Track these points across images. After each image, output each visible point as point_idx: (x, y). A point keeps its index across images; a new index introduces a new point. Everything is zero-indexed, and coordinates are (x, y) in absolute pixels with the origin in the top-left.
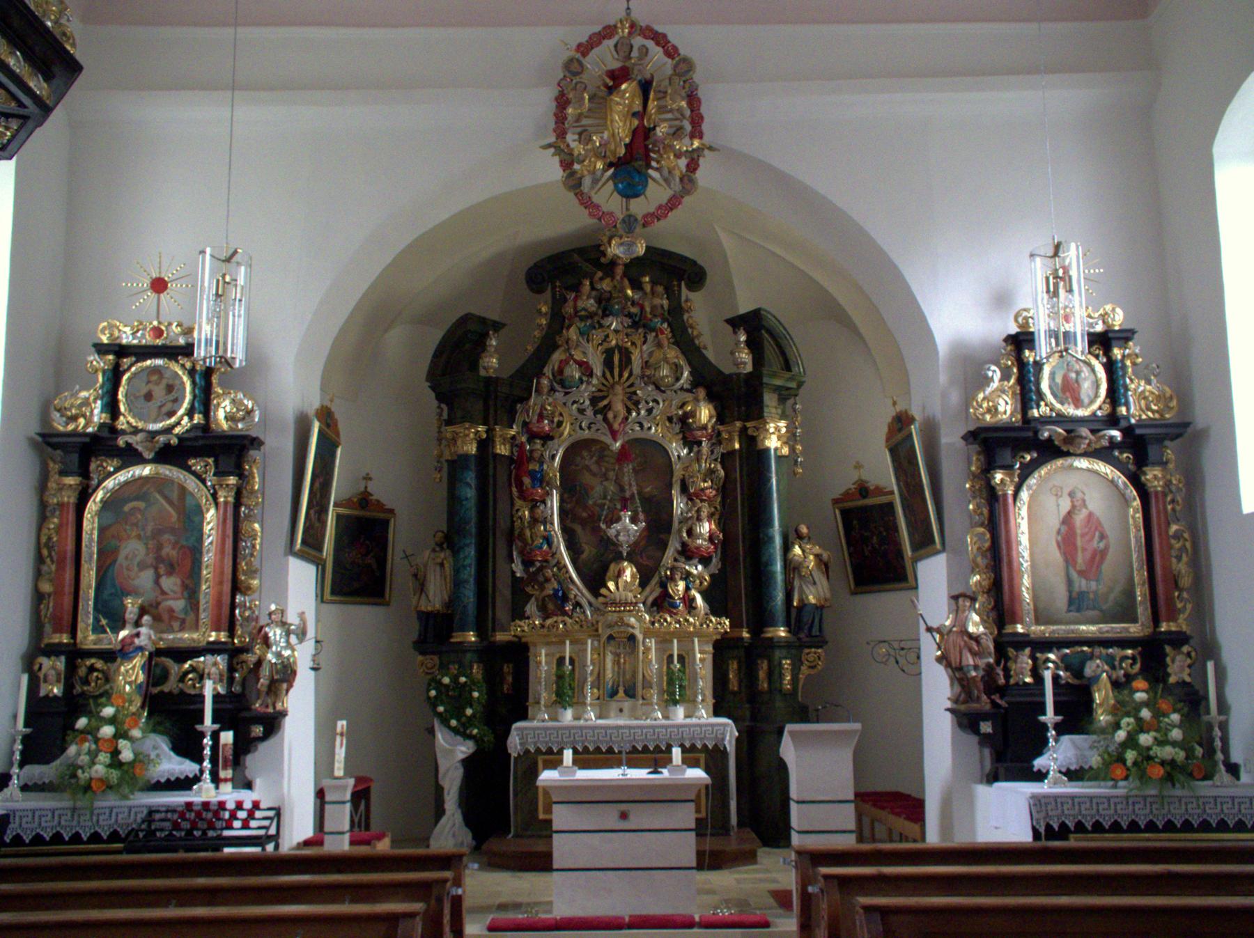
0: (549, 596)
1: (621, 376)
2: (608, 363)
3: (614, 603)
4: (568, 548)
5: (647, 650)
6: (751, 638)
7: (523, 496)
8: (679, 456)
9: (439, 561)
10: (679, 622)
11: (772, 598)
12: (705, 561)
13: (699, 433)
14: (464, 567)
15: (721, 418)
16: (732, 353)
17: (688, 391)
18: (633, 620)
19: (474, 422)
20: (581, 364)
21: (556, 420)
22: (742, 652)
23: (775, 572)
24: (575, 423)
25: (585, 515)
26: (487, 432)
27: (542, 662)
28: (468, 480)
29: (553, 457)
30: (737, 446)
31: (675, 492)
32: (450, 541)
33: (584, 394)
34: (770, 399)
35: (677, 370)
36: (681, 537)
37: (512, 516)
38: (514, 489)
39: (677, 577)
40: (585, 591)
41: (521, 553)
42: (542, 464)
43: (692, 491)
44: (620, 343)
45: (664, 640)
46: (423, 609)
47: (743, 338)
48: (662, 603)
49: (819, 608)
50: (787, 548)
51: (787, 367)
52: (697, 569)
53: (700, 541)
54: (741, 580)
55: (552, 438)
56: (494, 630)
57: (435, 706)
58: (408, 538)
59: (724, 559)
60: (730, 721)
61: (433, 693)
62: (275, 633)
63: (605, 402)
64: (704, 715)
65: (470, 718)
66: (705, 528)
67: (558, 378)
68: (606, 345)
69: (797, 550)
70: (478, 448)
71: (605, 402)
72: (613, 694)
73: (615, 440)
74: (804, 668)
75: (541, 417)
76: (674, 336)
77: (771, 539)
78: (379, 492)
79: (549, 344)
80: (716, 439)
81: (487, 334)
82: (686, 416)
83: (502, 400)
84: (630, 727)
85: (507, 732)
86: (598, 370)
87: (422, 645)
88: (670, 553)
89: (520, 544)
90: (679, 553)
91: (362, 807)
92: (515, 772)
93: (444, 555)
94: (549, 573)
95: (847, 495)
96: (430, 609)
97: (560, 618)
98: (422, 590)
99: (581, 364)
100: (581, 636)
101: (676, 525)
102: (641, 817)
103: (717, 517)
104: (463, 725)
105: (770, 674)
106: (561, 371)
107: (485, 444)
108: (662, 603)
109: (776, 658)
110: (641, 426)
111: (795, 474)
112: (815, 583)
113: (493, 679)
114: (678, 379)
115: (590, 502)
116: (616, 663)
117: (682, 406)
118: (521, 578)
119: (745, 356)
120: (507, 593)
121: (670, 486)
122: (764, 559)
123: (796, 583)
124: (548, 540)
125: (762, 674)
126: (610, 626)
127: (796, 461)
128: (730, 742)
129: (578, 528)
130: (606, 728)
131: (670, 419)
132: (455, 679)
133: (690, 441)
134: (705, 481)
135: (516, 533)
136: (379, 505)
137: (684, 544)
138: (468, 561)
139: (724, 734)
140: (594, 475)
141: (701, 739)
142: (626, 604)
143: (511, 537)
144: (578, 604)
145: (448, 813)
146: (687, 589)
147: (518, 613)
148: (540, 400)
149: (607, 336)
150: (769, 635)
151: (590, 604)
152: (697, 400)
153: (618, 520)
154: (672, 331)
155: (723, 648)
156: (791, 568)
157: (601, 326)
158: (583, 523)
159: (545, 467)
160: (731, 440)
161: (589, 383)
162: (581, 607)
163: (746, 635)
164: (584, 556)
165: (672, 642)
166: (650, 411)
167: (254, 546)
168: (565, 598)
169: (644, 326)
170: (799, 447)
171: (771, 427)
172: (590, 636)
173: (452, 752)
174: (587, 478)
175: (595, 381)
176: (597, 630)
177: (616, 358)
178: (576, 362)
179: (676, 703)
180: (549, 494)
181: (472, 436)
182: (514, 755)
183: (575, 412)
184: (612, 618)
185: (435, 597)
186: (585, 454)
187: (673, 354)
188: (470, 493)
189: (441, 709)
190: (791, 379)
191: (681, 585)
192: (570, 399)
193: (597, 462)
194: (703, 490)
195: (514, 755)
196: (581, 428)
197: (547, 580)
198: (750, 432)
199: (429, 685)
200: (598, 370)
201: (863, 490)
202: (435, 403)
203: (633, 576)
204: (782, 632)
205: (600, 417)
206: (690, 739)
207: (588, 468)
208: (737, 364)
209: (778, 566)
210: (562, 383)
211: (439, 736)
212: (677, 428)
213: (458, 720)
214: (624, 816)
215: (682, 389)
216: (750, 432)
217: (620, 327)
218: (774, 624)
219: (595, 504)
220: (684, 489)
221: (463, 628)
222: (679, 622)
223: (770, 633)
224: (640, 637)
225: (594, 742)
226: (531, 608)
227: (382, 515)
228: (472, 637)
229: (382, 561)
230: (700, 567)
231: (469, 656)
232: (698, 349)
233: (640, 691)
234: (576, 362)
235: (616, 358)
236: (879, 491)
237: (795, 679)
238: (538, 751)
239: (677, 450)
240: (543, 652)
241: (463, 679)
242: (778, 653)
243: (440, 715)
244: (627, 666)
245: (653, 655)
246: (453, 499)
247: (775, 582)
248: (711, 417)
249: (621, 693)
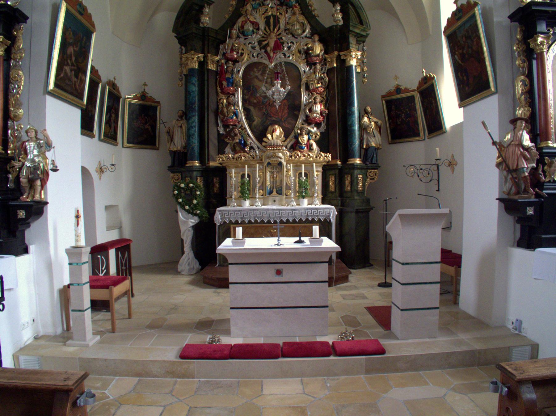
0: (237, 143)
1: (274, 30)
2: (267, 23)
3: (271, 146)
4: (247, 119)
5: (288, 170)
6: (342, 164)
7: (223, 92)
8: (304, 71)
9: (180, 125)
10: (304, 156)
11: (352, 143)
12: (318, 125)
13: (315, 59)
14: (192, 127)
15: (326, 52)
16: (333, 15)
17: (308, 38)
18: (281, 155)
19: (197, 51)
20: (253, 23)
21: (240, 52)
22: (337, 171)
23: (354, 131)
24: (251, 54)
25: (255, 101)
26: (204, 57)
27: (233, 176)
28: (194, 82)
29: (239, 71)
30: (335, 65)
31: (303, 89)
32: (185, 115)
33: (255, 38)
34: (352, 40)
35: (303, 25)
36: (305, 113)
37: (217, 102)
38: (219, 89)
39: (304, 133)
40: (255, 141)
41: (222, 121)
42: (232, 74)
43: (312, 88)
44: (274, 14)
45: (297, 166)
46: (172, 150)
47: (339, 8)
48: (296, 146)
49: (377, 149)
50: (360, 118)
51: (361, 23)
52: (314, 130)
53: (315, 115)
54: (337, 134)
55: (238, 62)
56: (209, 161)
57: (177, 199)
58: (167, 115)
59: (327, 124)
60: (333, 207)
61: (176, 192)
62: (31, 146)
63: (266, 42)
64: (318, 204)
65: (195, 205)
66: (318, 108)
67: (241, 30)
68: (266, 15)
69: (366, 119)
70: (199, 66)
71: (266, 42)
72: (271, 192)
73: (271, 63)
74: (368, 180)
75: (232, 50)
76: (301, 10)
77: (352, 113)
78: (151, 92)
79: (236, 14)
80: (324, 62)
81: (204, 6)
82: (308, 49)
83: (212, 41)
84: (279, 210)
85: (214, 213)
86: (262, 26)
87: (172, 169)
88: (300, 121)
89: (221, 116)
90: (304, 121)
91: (126, 255)
92: (219, 234)
93: (183, 122)
94: (237, 131)
95: (390, 94)
96: (175, 149)
97: (242, 154)
98: (172, 141)
99: (253, 23)
100: (253, 163)
101: (303, 107)
102: (290, 273)
103: (324, 102)
104: (192, 208)
105: (352, 183)
106: (242, 27)
107: (203, 64)
108: (296, 146)
109: (355, 174)
110: (285, 55)
111: (363, 82)
112: (374, 136)
113: (208, 185)
114: (304, 32)
115: (258, 95)
116: (272, 177)
117: (306, 45)
118: (223, 134)
119: (340, 16)
120: (216, 142)
121: (300, 87)
122: (349, 123)
123: (365, 136)
124: (236, 114)
125: (347, 182)
126: (269, 158)
127: (364, 76)
128: (333, 217)
129: (252, 108)
130: (267, 210)
131: (300, 52)
132: (187, 185)
133: (311, 64)
134: (318, 83)
135: (219, 111)
136: (151, 99)
137: (307, 117)
138: (194, 124)
139: (330, 213)
140: (260, 80)
141: (317, 216)
142: (277, 146)
143: (217, 113)
144: (251, 148)
145: (185, 253)
146: (309, 139)
147: (221, 151)
148: (231, 42)
149: (267, 10)
150: (350, 163)
151: (258, 148)
152: (314, 42)
153: (273, 85)
154: (301, 8)
155: (327, 169)
156: (363, 128)
157: (264, 5)
158: (255, 105)
159: (234, 76)
160: (332, 62)
161: (257, 33)
162: (254, 149)
163: (339, 163)
164: (255, 123)
165: (301, 166)
166: (289, 48)
167: (19, 87)
168: (245, 145)
169: (286, 5)
170: (365, 69)
171: (353, 54)
172: (258, 163)
173: (186, 223)
174: (257, 83)
175: (260, 33)
176: (262, 160)
177: (272, 20)
178: (251, 22)
179: (303, 197)
180: (236, 91)
181: (195, 59)
182: (218, 224)
183: (250, 49)
184: (269, 153)
185: (178, 143)
186: (255, 70)
187: (302, 19)
188: (195, 89)
189: (180, 200)
190: (364, 30)
191: (306, 137)
192: (248, 41)
193: (262, 74)
194: (317, 88)
195: (218, 224)
196: (253, 56)
197: (236, 135)
198: (342, 57)
199: (174, 188)
200: (262, 26)
201: (398, 90)
202: (179, 46)
203: (281, 133)
204: (358, 161)
205: (263, 51)
206: (312, 216)
207: (257, 77)
208: (336, 21)
209: (356, 127)
210: (243, 33)
211: (180, 214)
212: (304, 56)
213: (189, 206)
214: (279, 272)
215: (306, 37)
216: (342, 57)
217: (274, 6)
218: (353, 157)
219: (260, 96)
220: (307, 88)
221: (192, 159)
222: (304, 156)
223: (351, 161)
224: (284, 163)
225: (261, 218)
226: (228, 149)
227: (153, 104)
228: (197, 164)
229: (154, 127)
230: (315, 129)
231: (195, 173)
232: (314, 17)
233: (284, 191)
234: (251, 22)
235: (272, 20)
236: (407, 90)
237: (364, 185)
238: (231, 222)
239: (303, 68)
240: (233, 171)
241: (191, 185)
242: (356, 172)
243: (180, 203)
244: (278, 178)
245: (291, 173)
246: (187, 93)
247: (355, 135)
248: (321, 50)
249: (275, 193)
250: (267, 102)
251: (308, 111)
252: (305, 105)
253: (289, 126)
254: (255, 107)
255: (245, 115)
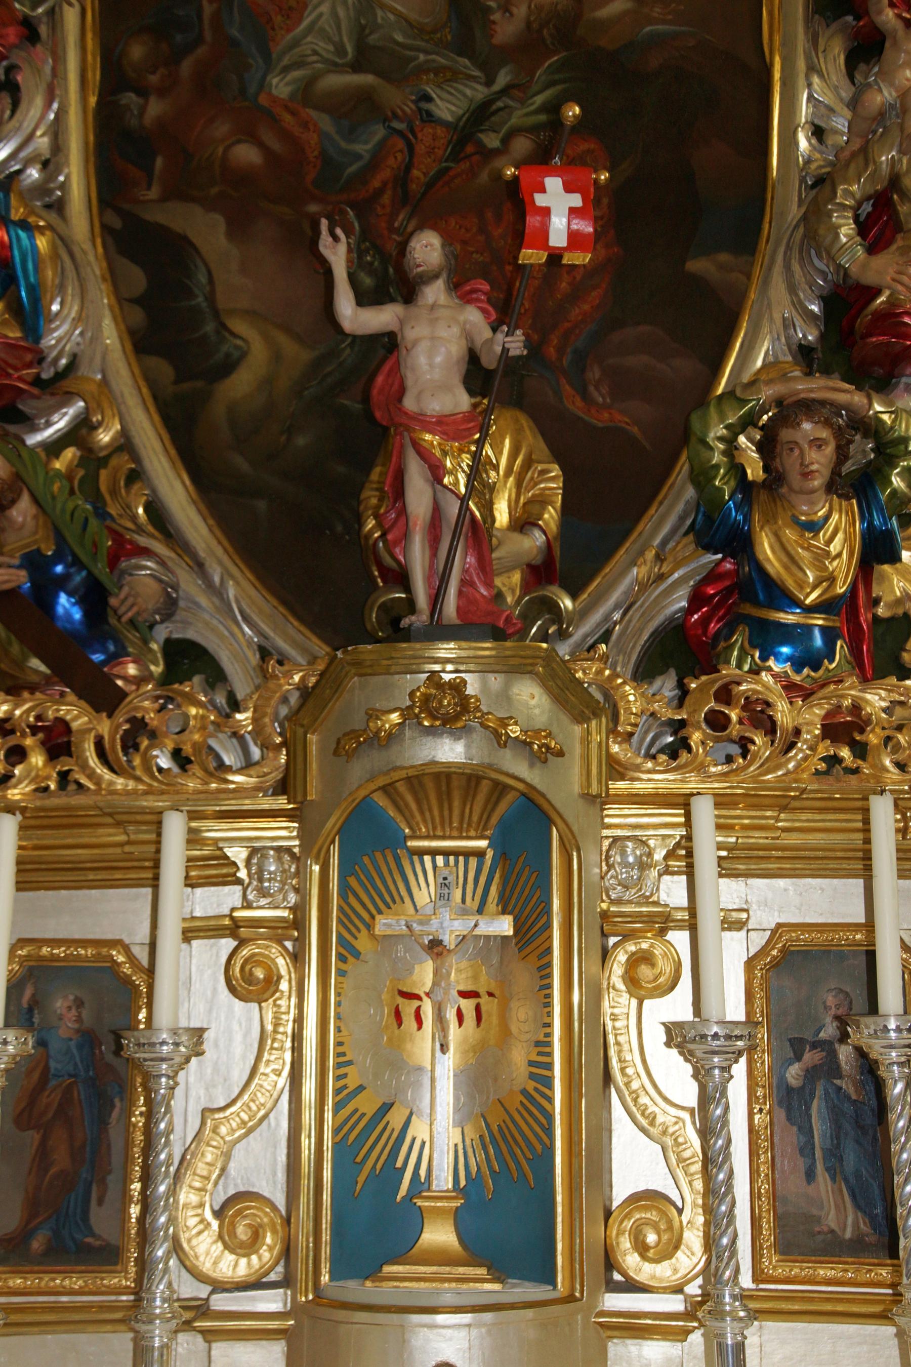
4: (141, 343)
25: (247, 154)
88: (760, 351)
101: (787, 206)
115: (281, 86)
158: (241, 200)
162: (216, 676)
164: (241, 384)
219: (306, 93)
250: (375, 162)
251: (846, 231)
252: (822, 184)
253: (629, 417)
254: (239, 226)
255: (122, 300)
